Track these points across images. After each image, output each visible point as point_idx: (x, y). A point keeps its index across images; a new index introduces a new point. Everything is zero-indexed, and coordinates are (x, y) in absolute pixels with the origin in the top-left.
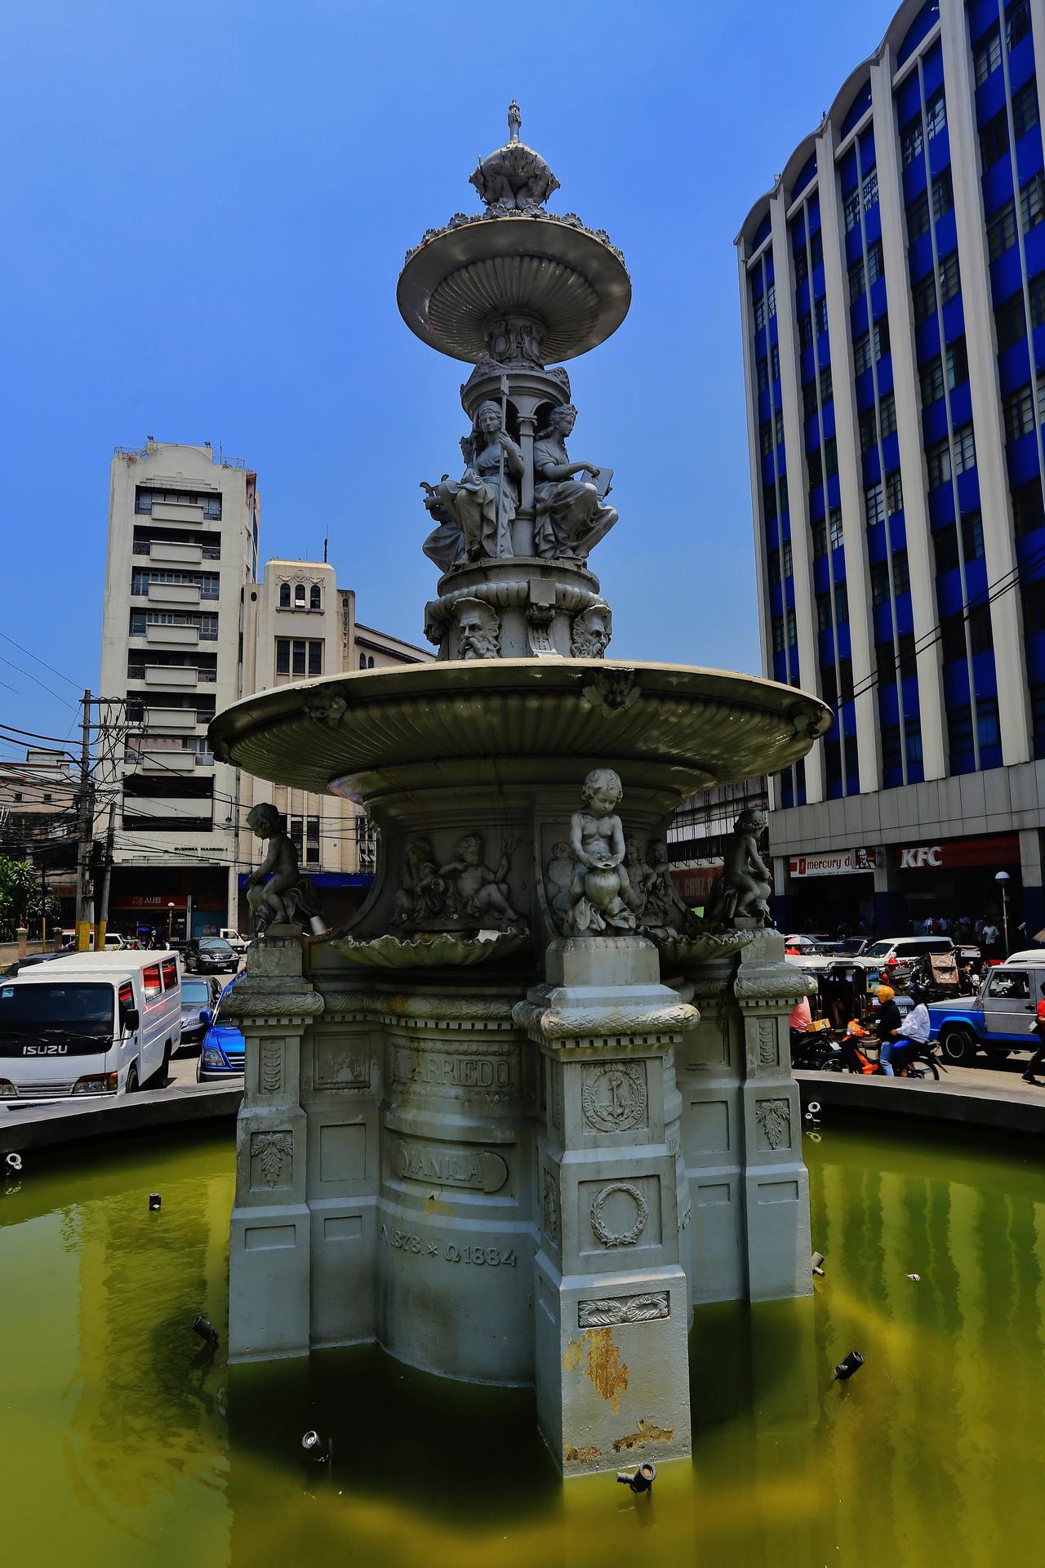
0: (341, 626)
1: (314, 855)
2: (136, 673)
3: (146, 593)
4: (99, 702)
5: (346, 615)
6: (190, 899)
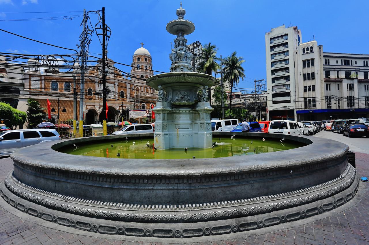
0: (319, 54)
1: (314, 106)
2: (273, 74)
3: (274, 59)
5: (320, 51)
6: (287, 116)
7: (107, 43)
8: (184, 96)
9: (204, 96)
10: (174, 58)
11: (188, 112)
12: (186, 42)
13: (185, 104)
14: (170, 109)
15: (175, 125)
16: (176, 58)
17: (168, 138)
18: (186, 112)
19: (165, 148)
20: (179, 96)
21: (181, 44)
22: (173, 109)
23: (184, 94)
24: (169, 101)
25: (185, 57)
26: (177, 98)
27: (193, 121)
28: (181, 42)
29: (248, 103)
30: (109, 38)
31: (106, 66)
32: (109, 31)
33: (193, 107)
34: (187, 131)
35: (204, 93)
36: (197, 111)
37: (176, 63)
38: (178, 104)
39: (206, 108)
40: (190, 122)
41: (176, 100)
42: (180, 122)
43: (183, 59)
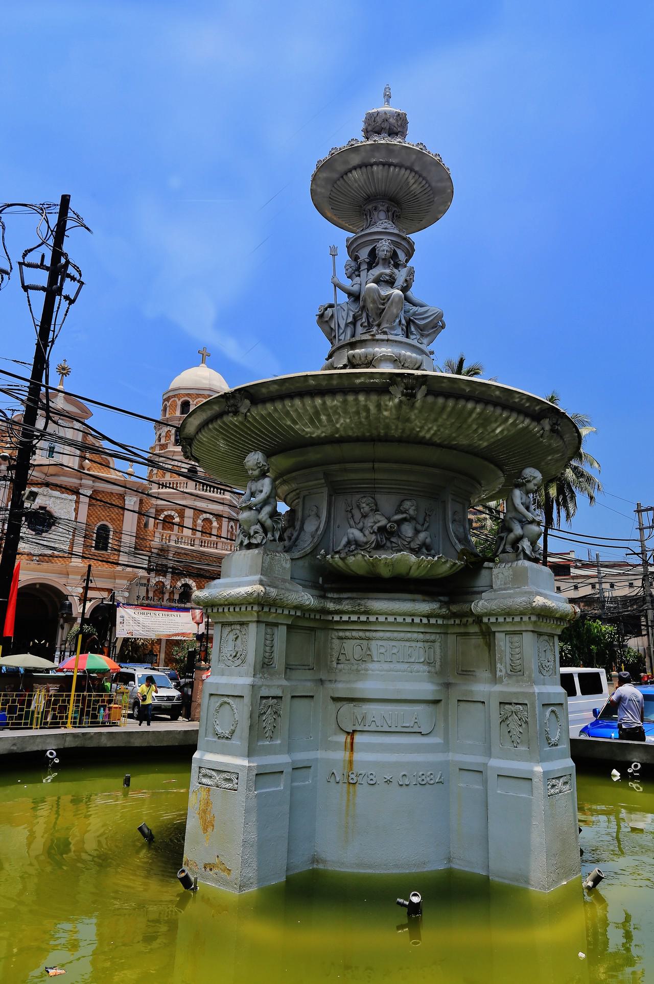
4: (647, 510)
7: (59, 321)
8: (400, 523)
9: (518, 530)
10: (342, 326)
11: (417, 620)
12: (409, 254)
13: (402, 570)
14: (307, 598)
15: (339, 704)
16: (354, 323)
17: (283, 796)
18: (409, 620)
19: (260, 880)
20: (369, 522)
22: (324, 597)
23: (399, 511)
24: (308, 549)
25: (403, 322)
26: (353, 536)
27: (447, 685)
28: (384, 247)
29: (614, 600)
30: (70, 304)
31: (39, 412)
32: (73, 279)
33: (452, 590)
34: (418, 749)
35: (522, 509)
36: (478, 619)
37: (352, 345)
38: (361, 572)
39: (539, 601)
40: (427, 688)
41: (349, 543)
42: (368, 686)
43: (392, 328)
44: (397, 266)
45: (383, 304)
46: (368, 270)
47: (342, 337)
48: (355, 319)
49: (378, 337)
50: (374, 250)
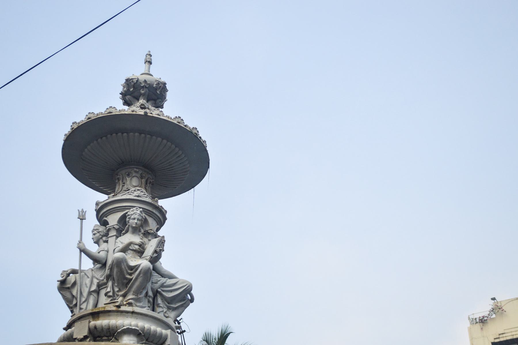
16: (97, 292)
21: (133, 222)
25: (150, 293)
37: (95, 315)
44: (147, 234)
45: (131, 274)
46: (117, 237)
47: (84, 306)
48: (100, 286)
49: (123, 308)
50: (124, 217)
